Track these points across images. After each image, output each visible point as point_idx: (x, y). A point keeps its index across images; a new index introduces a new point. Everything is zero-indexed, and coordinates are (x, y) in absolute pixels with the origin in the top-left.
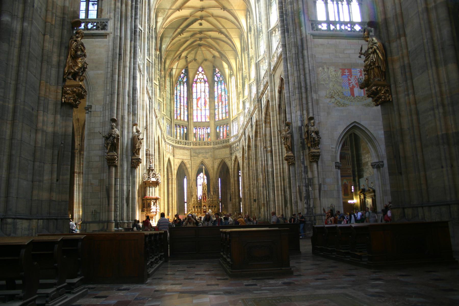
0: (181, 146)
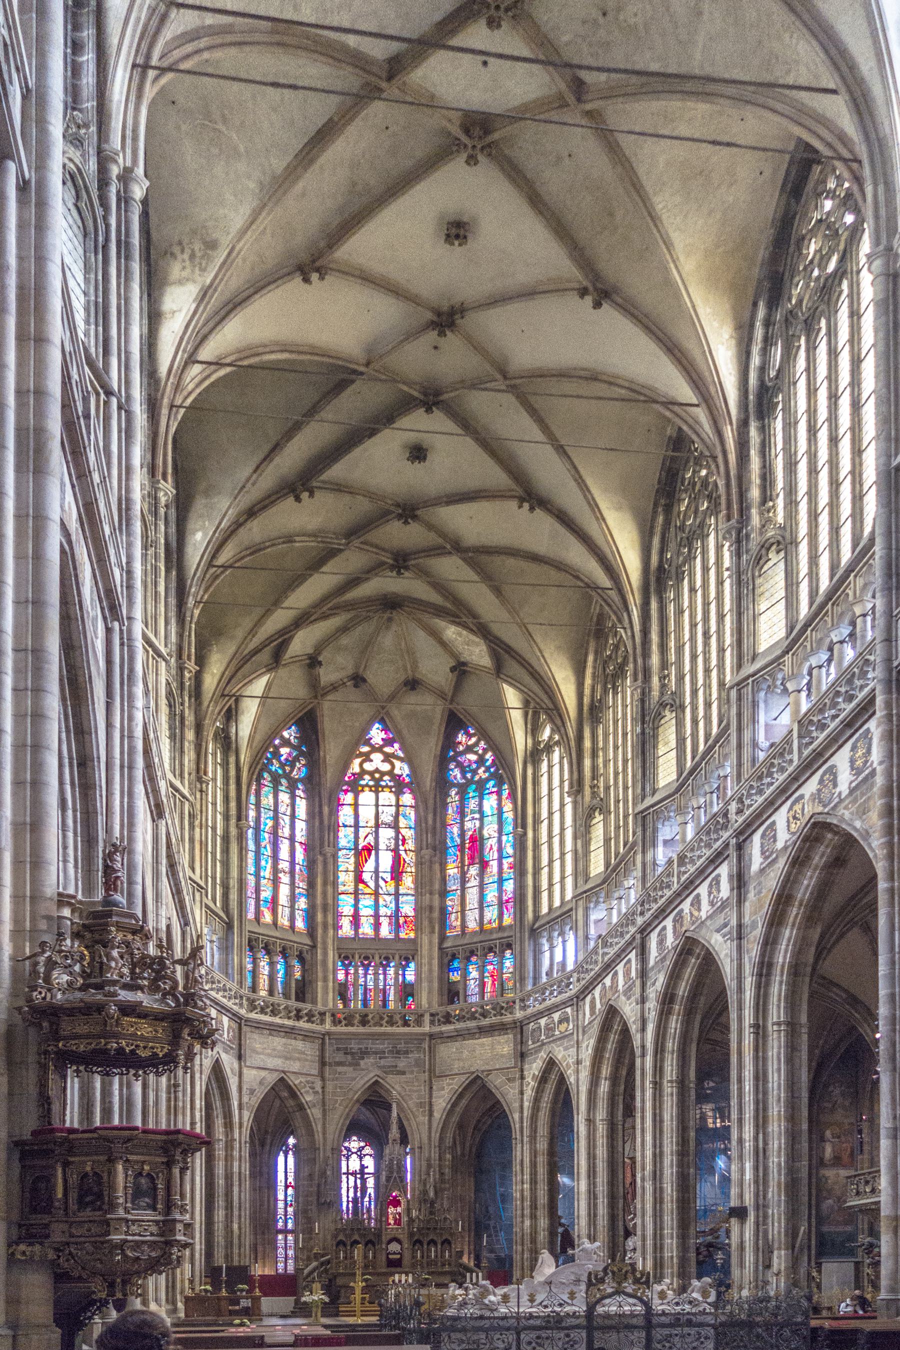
0: (277, 1020)
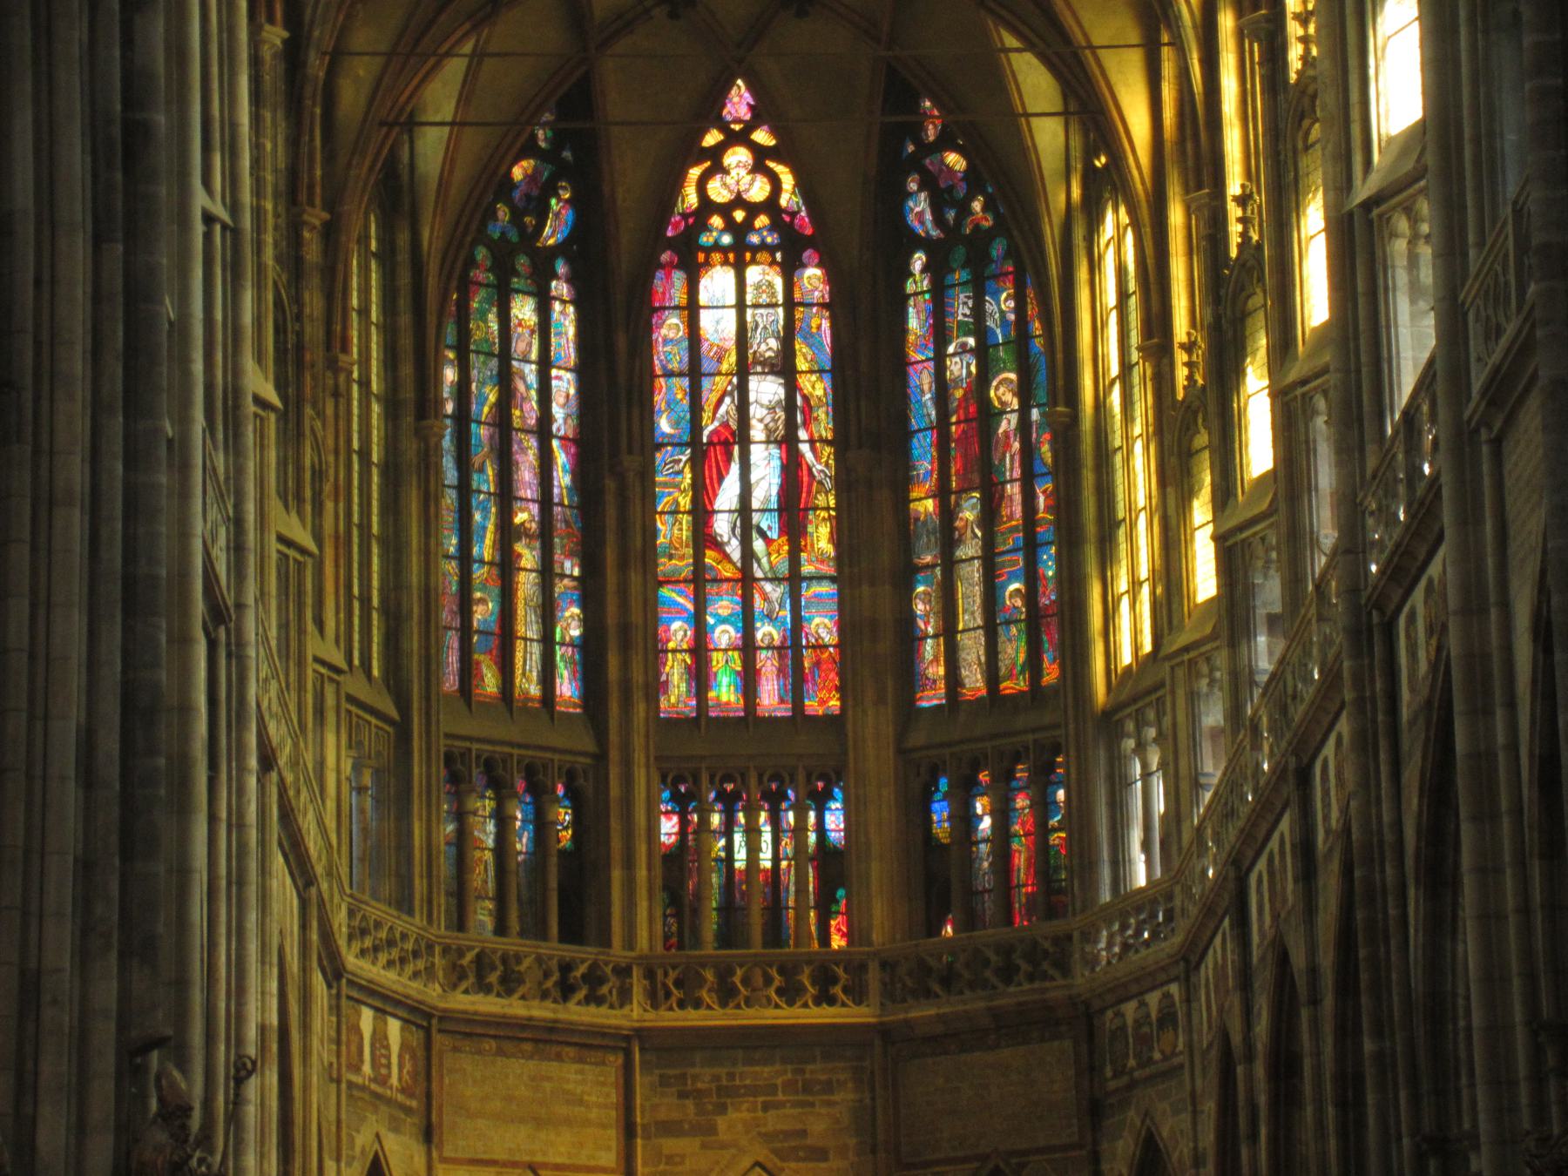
0: (515, 1007)
